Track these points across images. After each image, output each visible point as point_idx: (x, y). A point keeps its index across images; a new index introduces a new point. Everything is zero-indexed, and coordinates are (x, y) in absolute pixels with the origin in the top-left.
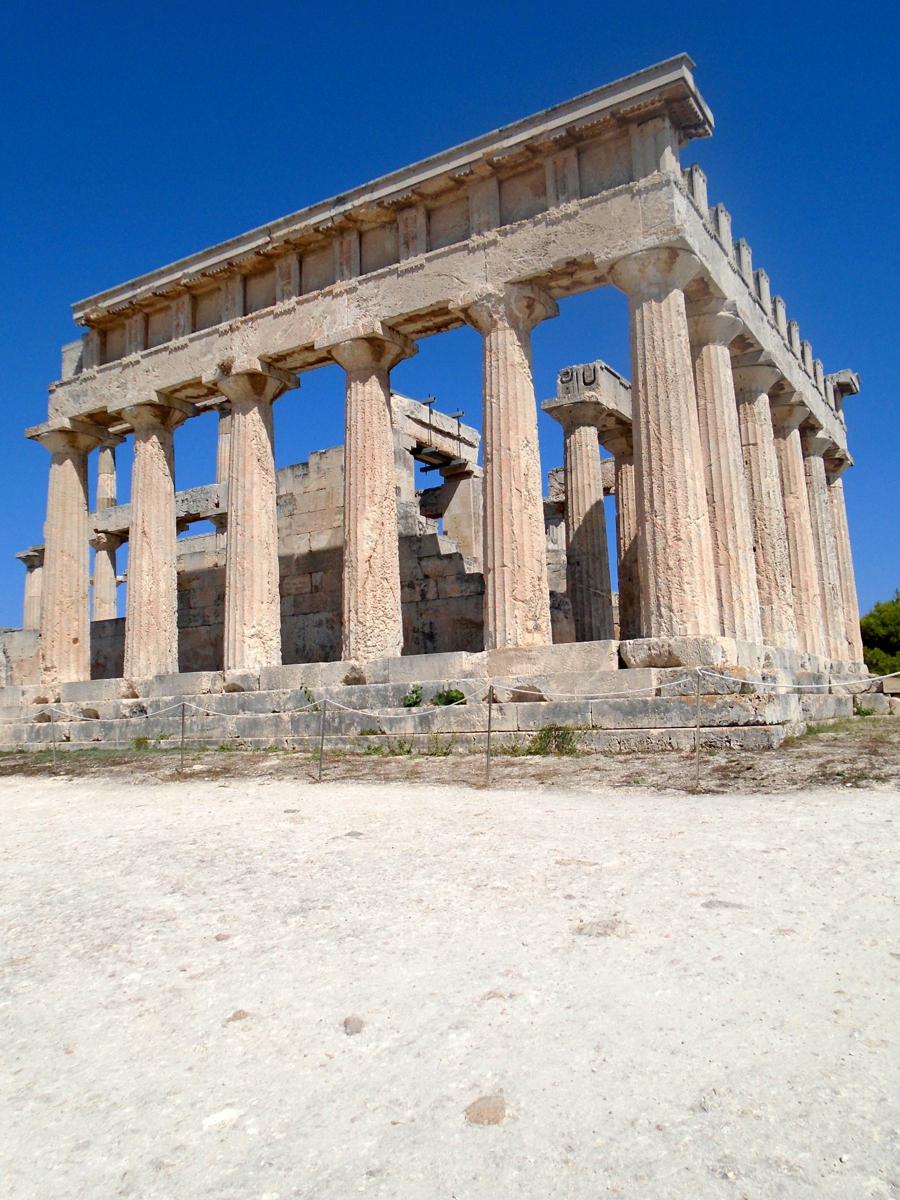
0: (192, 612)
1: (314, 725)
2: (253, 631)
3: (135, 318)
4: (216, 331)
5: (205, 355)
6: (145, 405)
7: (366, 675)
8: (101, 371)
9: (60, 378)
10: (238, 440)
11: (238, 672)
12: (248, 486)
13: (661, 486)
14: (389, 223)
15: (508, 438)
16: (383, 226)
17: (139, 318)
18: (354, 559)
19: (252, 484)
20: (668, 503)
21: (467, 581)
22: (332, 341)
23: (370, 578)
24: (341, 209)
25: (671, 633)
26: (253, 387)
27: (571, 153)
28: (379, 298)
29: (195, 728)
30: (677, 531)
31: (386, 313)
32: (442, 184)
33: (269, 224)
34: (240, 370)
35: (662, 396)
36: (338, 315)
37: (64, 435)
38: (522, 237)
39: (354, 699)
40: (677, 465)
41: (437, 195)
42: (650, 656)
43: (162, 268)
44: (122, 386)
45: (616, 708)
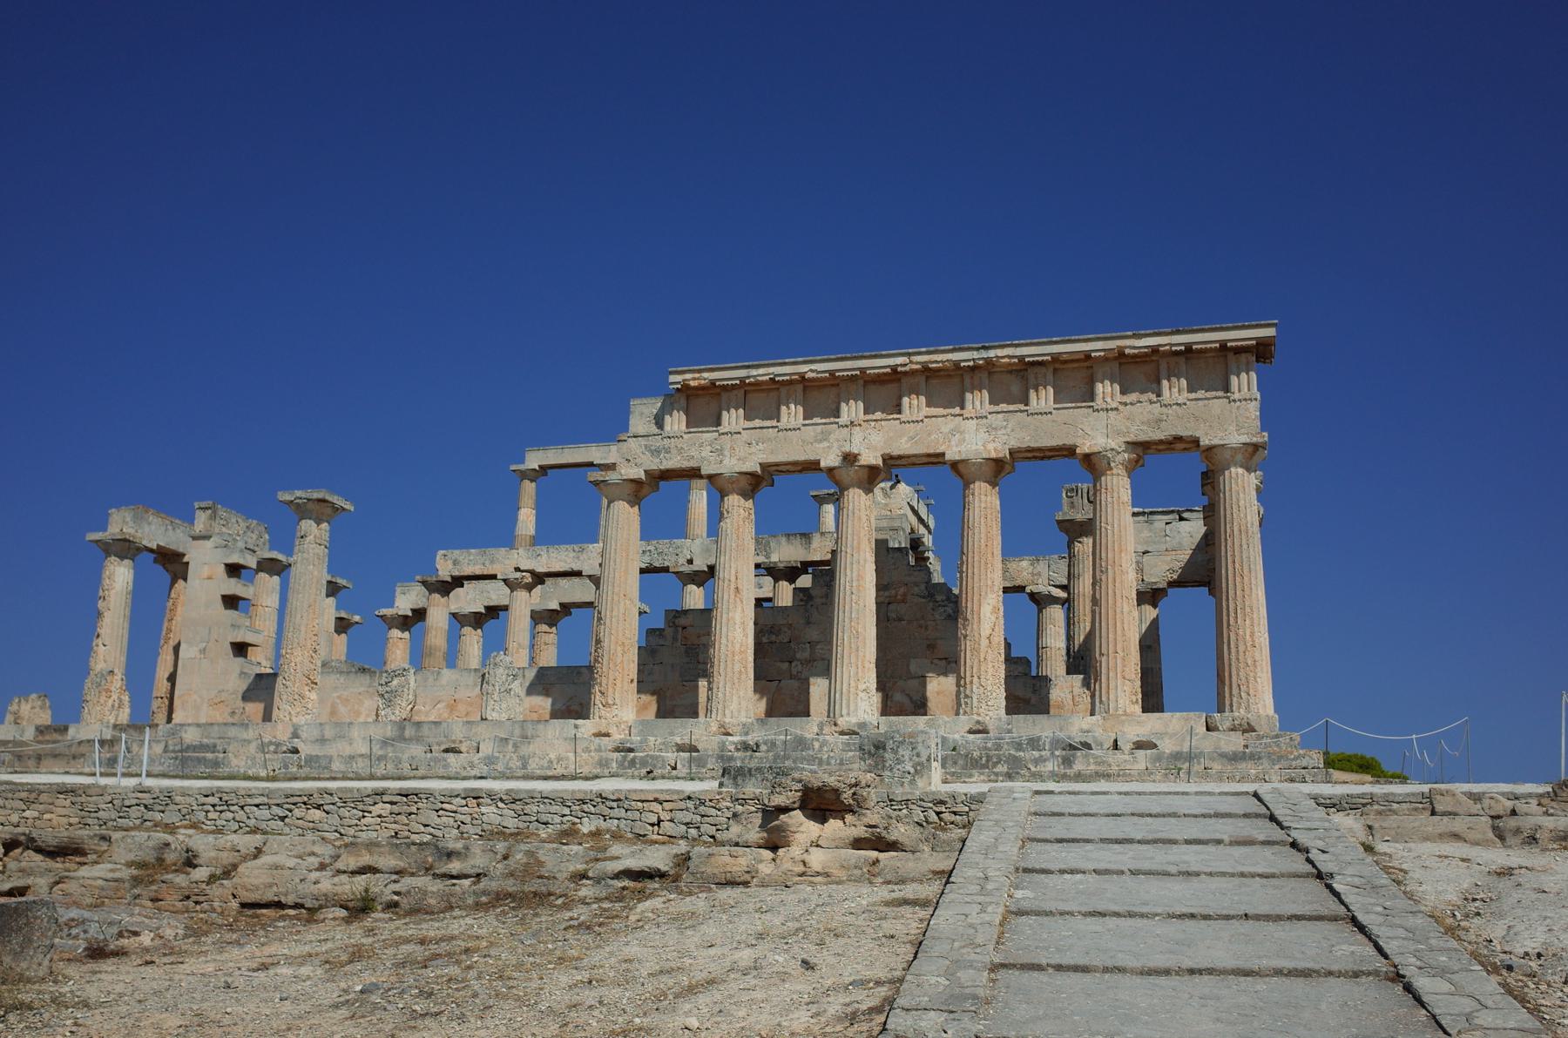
0: (700, 666)
1: (961, 762)
2: (864, 687)
3: (735, 392)
4: (837, 423)
5: (820, 441)
6: (746, 473)
7: (990, 727)
8: (690, 433)
9: (627, 430)
10: (853, 521)
11: (854, 720)
12: (862, 562)
13: (1243, 609)
14: (1016, 370)
15: (1121, 558)
16: (1011, 372)
17: (743, 392)
18: (976, 634)
19: (865, 561)
20: (1248, 622)
21: (1015, 663)
22: (963, 457)
23: (990, 651)
24: (984, 354)
25: (1248, 708)
26: (869, 477)
27: (1182, 360)
28: (1009, 430)
29: (833, 762)
30: (1253, 641)
31: (1014, 443)
32: (1077, 357)
33: (910, 351)
34: (865, 463)
35: (1245, 546)
36: (967, 436)
37: (633, 485)
38: (1140, 411)
39: (989, 745)
40: (1254, 595)
41: (1066, 362)
42: (1234, 725)
43: (787, 360)
44: (720, 452)
45: (1223, 755)
